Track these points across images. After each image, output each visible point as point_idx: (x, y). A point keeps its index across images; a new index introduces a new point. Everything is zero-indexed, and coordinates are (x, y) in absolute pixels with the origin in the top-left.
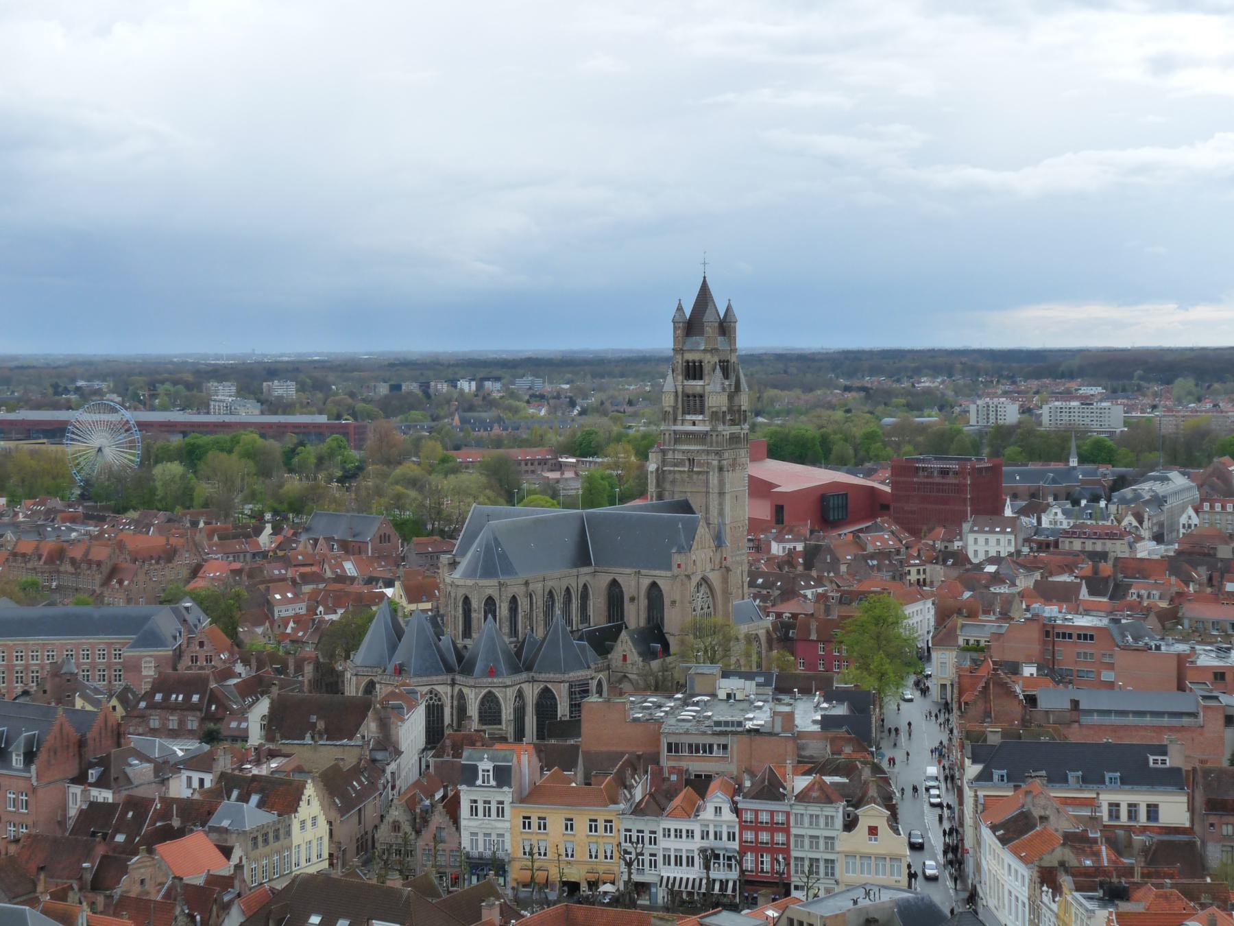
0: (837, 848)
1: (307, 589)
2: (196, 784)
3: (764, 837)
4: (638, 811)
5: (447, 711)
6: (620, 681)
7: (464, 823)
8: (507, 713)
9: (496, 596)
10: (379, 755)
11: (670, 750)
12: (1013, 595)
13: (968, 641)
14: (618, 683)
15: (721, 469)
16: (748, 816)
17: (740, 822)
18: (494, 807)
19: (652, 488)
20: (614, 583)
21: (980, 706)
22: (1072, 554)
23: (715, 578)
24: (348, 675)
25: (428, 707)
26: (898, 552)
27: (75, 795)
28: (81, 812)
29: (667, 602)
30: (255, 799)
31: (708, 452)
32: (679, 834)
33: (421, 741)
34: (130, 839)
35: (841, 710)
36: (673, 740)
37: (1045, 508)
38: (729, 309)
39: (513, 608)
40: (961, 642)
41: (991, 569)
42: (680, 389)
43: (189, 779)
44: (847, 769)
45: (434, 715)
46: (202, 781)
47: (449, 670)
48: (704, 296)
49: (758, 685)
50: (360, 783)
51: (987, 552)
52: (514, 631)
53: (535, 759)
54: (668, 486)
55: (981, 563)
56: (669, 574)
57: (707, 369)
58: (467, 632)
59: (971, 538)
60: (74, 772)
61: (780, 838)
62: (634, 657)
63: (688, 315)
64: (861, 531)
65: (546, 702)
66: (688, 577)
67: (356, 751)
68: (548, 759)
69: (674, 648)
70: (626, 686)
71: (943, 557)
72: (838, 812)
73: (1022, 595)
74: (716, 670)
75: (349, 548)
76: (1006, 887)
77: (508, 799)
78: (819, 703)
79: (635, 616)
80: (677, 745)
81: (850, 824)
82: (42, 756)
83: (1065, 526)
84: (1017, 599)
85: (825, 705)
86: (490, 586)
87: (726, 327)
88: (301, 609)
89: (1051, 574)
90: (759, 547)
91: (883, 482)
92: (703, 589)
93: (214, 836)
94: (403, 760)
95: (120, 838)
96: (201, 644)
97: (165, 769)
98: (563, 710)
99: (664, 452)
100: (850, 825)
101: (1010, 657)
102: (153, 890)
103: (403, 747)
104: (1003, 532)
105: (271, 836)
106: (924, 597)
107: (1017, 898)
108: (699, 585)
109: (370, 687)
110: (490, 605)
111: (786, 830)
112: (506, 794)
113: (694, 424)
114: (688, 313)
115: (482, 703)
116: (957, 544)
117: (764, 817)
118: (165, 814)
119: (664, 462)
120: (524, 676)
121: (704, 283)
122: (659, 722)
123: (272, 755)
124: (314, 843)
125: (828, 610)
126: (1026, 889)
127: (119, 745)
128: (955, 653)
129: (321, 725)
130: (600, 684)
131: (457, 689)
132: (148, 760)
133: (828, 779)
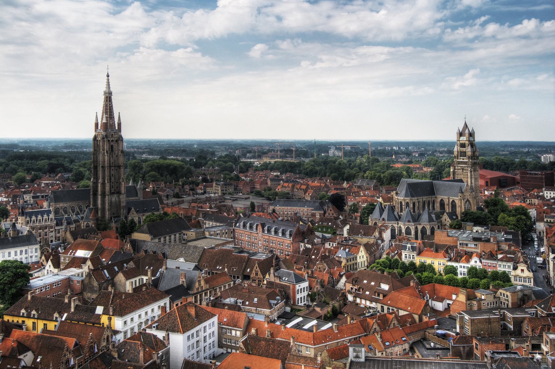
2: (331, 245)
4: (450, 260)
5: (397, 231)
13: (547, 220)
14: (442, 226)
18: (411, 256)
25: (391, 229)
27: (302, 245)
28: (303, 249)
29: (457, 206)
33: (390, 238)
34: (316, 257)
40: (545, 220)
41: (553, 201)
43: (330, 244)
44: (514, 253)
45: (393, 231)
46: (333, 244)
47: (397, 220)
50: (375, 248)
51: (550, 196)
65: (424, 231)
67: (373, 239)
69: (459, 218)
71: (538, 197)
74: (473, 224)
78: (503, 235)
79: (448, 209)
80: (462, 243)
94: (385, 243)
95: (313, 257)
98: (428, 232)
100: (515, 268)
103: (385, 239)
105: (352, 259)
109: (375, 224)
115: (406, 229)
116: (541, 194)
118: (325, 252)
124: (363, 263)
129: (363, 233)
130: (439, 226)
131: (399, 225)
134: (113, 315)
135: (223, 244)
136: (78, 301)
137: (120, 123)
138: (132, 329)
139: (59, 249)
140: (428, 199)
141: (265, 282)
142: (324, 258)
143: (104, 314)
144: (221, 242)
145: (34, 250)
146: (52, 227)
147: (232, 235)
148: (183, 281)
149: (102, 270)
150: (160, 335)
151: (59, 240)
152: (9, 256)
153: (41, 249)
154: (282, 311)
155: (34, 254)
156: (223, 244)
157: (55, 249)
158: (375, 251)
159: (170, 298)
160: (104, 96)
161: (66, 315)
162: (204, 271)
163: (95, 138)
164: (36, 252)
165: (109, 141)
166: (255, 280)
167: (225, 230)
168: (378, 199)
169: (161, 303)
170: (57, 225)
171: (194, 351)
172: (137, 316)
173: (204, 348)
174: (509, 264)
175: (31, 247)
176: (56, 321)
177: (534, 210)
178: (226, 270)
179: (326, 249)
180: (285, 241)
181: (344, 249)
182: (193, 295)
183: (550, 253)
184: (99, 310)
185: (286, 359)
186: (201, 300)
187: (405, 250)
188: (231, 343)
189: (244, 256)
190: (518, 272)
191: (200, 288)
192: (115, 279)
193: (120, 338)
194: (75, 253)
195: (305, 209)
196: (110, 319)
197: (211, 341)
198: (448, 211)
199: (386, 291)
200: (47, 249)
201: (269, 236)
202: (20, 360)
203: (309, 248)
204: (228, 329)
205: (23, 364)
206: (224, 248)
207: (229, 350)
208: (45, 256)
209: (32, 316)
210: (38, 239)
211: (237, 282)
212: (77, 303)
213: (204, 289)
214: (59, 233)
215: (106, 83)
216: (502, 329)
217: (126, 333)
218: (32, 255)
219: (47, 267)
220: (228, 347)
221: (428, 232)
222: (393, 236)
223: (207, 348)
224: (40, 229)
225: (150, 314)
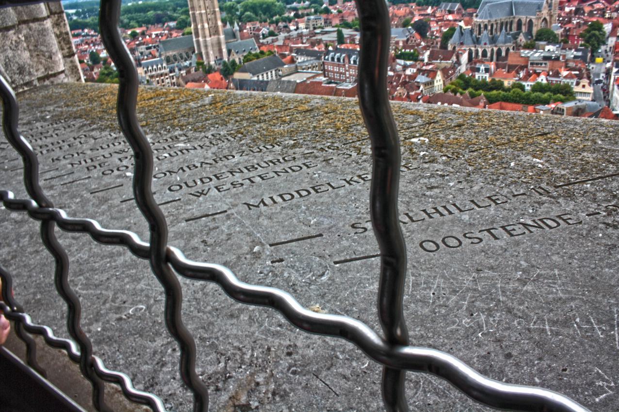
1: (439, 23)
8: (489, 54)
14: (517, 47)
35: (580, 54)
39: (492, 26)
52: (492, 34)
58: (480, 34)
62: (524, 40)
65: (499, 52)
70: (520, 48)
72: (574, 81)
88: (438, 28)
97: (405, 67)
98: (503, 54)
109: (454, 48)
118: (405, 78)
120: (494, 45)
122: (528, 57)
129: (442, 57)
135: (313, 77)
142: (404, 84)
146: (166, 74)
156: (313, 77)
158: (452, 74)
170: (171, 72)
179: (406, 75)
181: (423, 75)
189: (332, 87)
206: (315, 80)
214: (173, 79)
221: (503, 54)
222: (470, 59)
224: (157, 77)
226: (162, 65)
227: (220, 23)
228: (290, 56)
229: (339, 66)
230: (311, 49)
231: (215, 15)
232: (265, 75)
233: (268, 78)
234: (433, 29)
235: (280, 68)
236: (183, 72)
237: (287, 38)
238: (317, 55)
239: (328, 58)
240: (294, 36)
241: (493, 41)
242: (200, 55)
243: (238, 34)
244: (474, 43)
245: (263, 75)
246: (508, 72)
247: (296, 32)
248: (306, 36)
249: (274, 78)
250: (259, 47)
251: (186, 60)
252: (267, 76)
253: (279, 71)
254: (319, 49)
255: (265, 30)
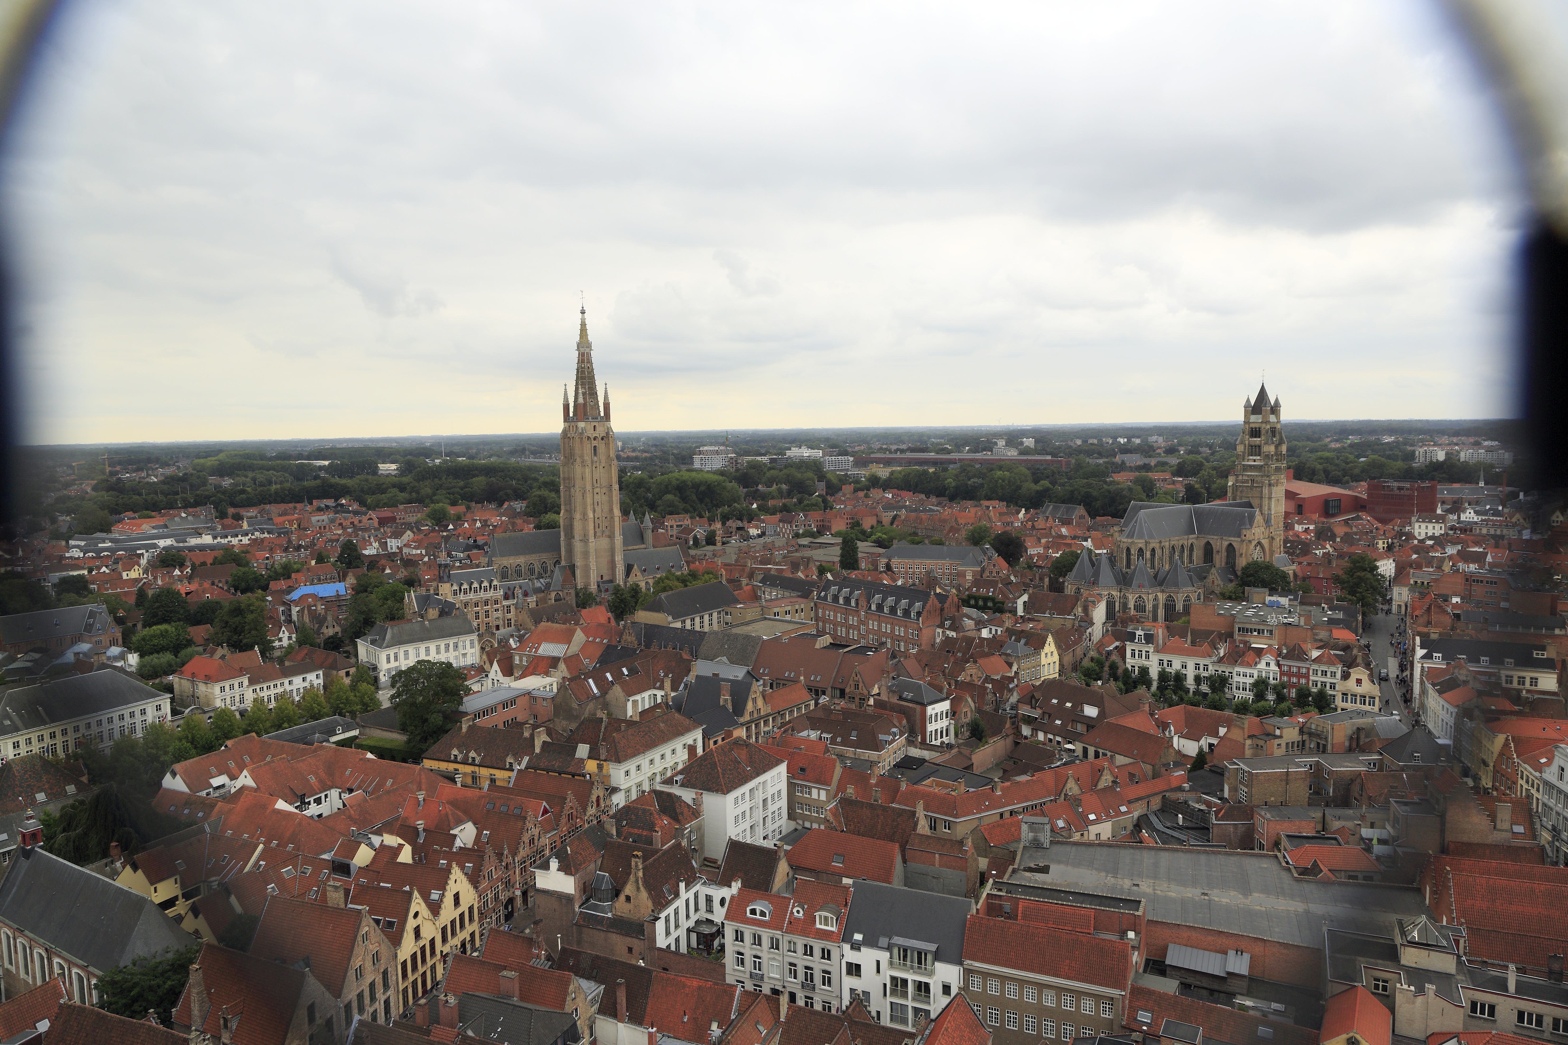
0: (1337, 688)
2: (993, 632)
3: (1294, 680)
5: (1117, 604)
6: (1210, 594)
7: (1127, 660)
8: (1149, 607)
9: (1144, 548)
10: (1083, 624)
11: (1239, 631)
12: (1444, 558)
15: (1270, 485)
16: (1286, 669)
17: (1281, 671)
19: (1229, 494)
20: (1208, 543)
21: (1425, 618)
22: (1480, 535)
23: (1265, 542)
24: (1066, 584)
26: (1371, 532)
30: (1023, 641)
31: (1262, 476)
32: (1245, 675)
33: (1104, 619)
35: (1340, 615)
36: (1241, 626)
37: (1464, 511)
38: (1277, 400)
42: (1247, 442)
43: (991, 629)
45: (1110, 606)
46: (996, 630)
48: (1262, 394)
49: (1290, 600)
52: (1153, 567)
53: (1165, 631)
54: (1239, 493)
55: (1423, 539)
56: (1239, 539)
57: (1263, 432)
58: (1128, 565)
59: (1417, 525)
60: (938, 623)
61: (1303, 681)
62: (1219, 582)
63: (1253, 403)
64: (1349, 519)
66: (1250, 541)
68: (1171, 631)
73: (1451, 557)
75: (1066, 522)
76: (1440, 717)
77: (1151, 650)
79: (1220, 560)
81: (1346, 676)
82: (924, 614)
83: (1475, 519)
84: (1447, 560)
85: (1330, 613)
86: (1141, 543)
87: (1275, 409)
89: (1468, 547)
90: (1288, 527)
91: (1360, 493)
92: (1258, 548)
93: (1003, 657)
94: (1095, 627)
95: (959, 654)
96: (994, 565)
98: (1180, 607)
99: (1237, 476)
101: (1443, 592)
102: (976, 680)
104: (1437, 522)
106: (1388, 557)
107: (1447, 723)
108: (1256, 546)
110: (1141, 551)
111: (1307, 676)
112: (1151, 648)
113: (1255, 461)
114: (1253, 403)
117: (1295, 670)
119: (1237, 481)
121: (1263, 387)
123: (1030, 620)
125: (1330, 562)
126: (1453, 719)
127: (958, 611)
128: (1407, 589)
130: (1199, 595)
132: (972, 619)
133: (1332, 652)
134: (605, 760)
136: (545, 735)
137: (609, 404)
138: (639, 785)
139: (511, 640)
140: (1181, 543)
141: (871, 702)
143: (589, 758)
144: (791, 627)
145: (468, 643)
146: (496, 602)
147: (812, 614)
148: (726, 700)
149: (586, 679)
150: (687, 795)
151: (509, 625)
152: (428, 654)
153: (479, 641)
154: (900, 756)
155: (469, 650)
157: (503, 643)
159: (703, 730)
160: (577, 352)
161: (526, 759)
162: (761, 682)
163: (565, 432)
164: (472, 647)
165: (589, 438)
166: (854, 698)
167: (800, 605)
168: (1084, 543)
169: (689, 739)
170: (506, 597)
171: (747, 825)
172: (647, 761)
173: (764, 819)
174: (1333, 669)
175: (463, 638)
176: (511, 769)
177: (1391, 561)
178: (802, 678)
180: (908, 624)
182: (742, 725)
183: (1418, 649)
184: (583, 750)
185: (907, 841)
186: (757, 734)
187: (1133, 641)
188: (810, 811)
190: (1351, 684)
191: (755, 712)
192: (608, 696)
193: (619, 800)
194: (537, 649)
195: (947, 562)
196: (600, 767)
197: (775, 807)
198: (1218, 565)
199: (1093, 718)
200: (490, 642)
201: (879, 616)
202: (455, 836)
203: (952, 638)
204: (806, 786)
205: (458, 843)
207: (807, 825)
208: (488, 654)
209: (470, 761)
210: (475, 624)
211: (821, 701)
212: (545, 738)
213: (762, 713)
214: (509, 612)
215: (579, 327)
216: (1310, 794)
217: (628, 791)
218: (465, 651)
219: (492, 675)
220: (805, 818)
223: (769, 820)
224: (476, 605)
225: (669, 762)
226: (491, 582)
227: (617, 512)
228: (749, 587)
229: (846, 613)
230: (791, 576)
231: (611, 497)
232: (697, 620)
233: (701, 627)
234: (1031, 551)
235: (729, 610)
236: (532, 600)
237: (743, 553)
238: (803, 589)
239: (826, 595)
240: (757, 549)
241: (1159, 581)
242: (572, 568)
243: (649, 535)
244: (1118, 583)
245: (693, 620)
246: (1193, 643)
247: (761, 540)
248: (780, 549)
249: (715, 627)
250: (688, 562)
251: (540, 576)
252: (702, 622)
253: (727, 614)
254: (807, 576)
255: (700, 532)
